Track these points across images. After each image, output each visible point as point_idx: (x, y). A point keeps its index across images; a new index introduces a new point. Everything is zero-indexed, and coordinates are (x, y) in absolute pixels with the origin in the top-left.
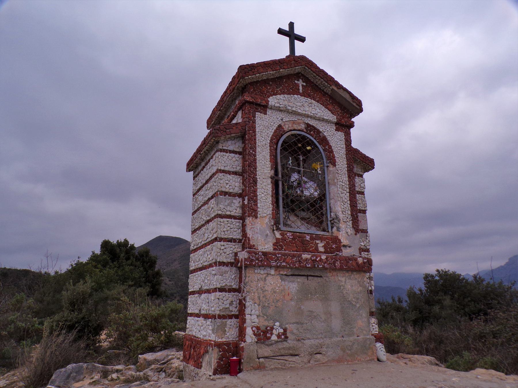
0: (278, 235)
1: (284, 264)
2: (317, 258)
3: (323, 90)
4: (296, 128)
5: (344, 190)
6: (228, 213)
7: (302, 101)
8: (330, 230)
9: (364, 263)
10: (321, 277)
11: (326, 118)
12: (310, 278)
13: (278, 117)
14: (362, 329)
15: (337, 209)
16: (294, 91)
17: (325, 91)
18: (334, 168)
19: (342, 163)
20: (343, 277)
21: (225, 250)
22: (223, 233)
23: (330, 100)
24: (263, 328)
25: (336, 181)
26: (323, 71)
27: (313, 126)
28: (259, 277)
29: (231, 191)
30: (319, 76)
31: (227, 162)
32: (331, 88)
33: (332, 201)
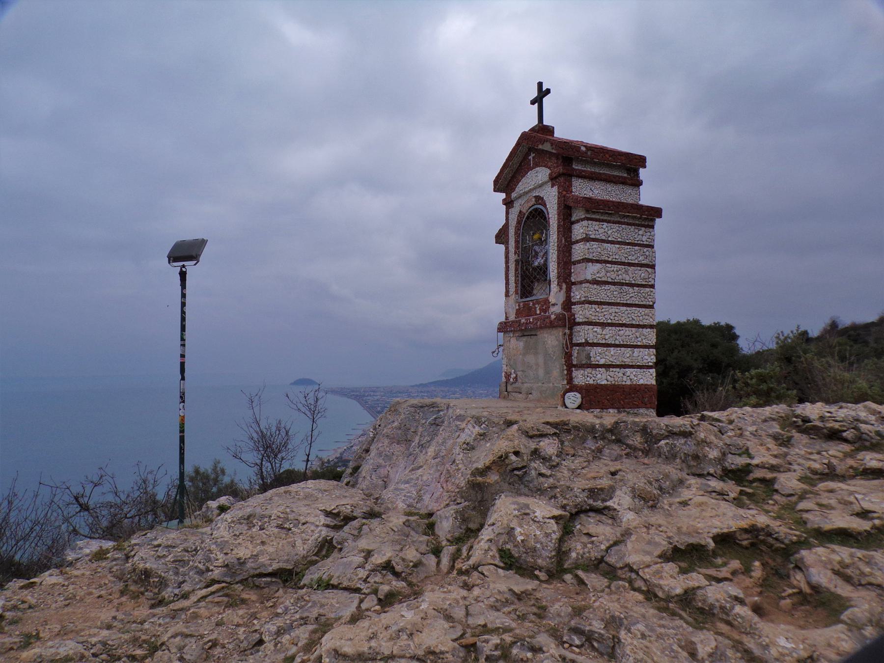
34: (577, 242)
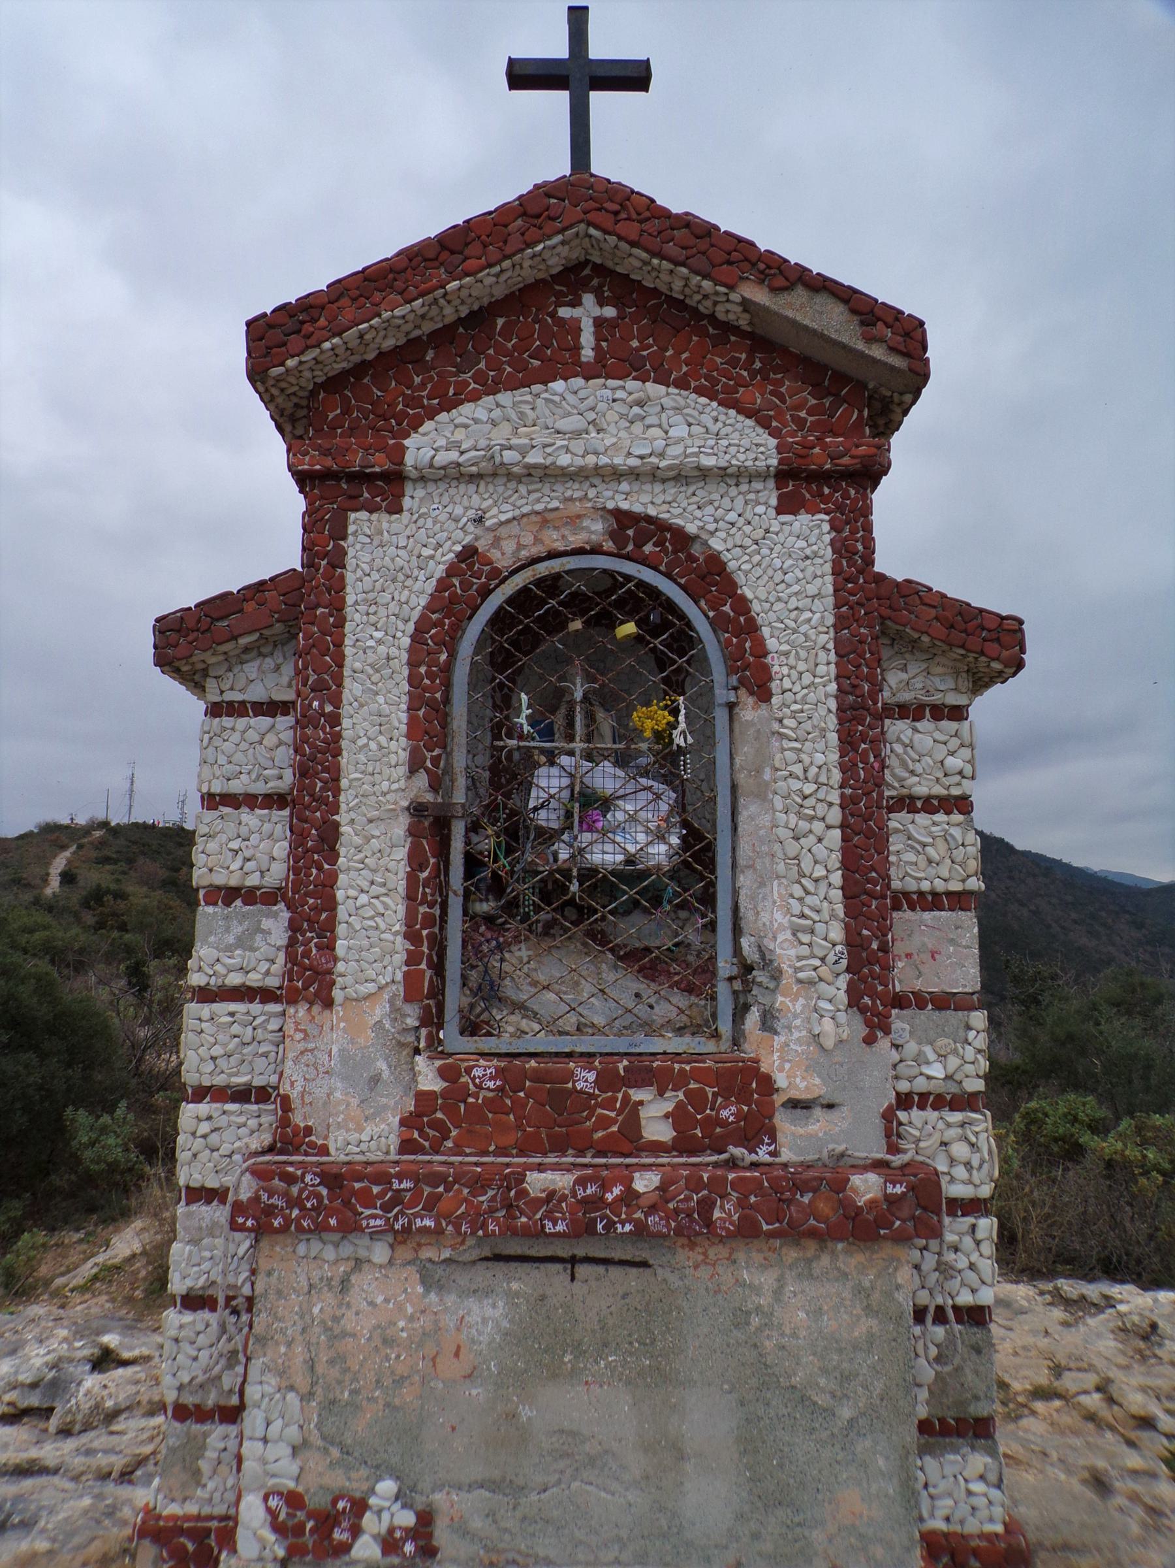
0: (429, 1080)
1: (428, 1222)
2: (605, 1186)
3: (712, 318)
4: (560, 546)
5: (812, 818)
6: (235, 979)
7: (590, 402)
8: (725, 1027)
9: (891, 1200)
10: (644, 1264)
11: (708, 461)
12: (582, 1270)
13: (458, 511)
14: (861, 1536)
15: (765, 917)
16: (559, 361)
17: (721, 316)
18: (763, 711)
19: (807, 679)
20: (763, 1268)
21: (214, 1138)
22: (209, 1067)
23: (751, 360)
24: (316, 1501)
25: (767, 775)
26: (687, 222)
27: (649, 519)
28: (316, 1275)
29: (253, 880)
30: (663, 257)
31: (239, 757)
32: (735, 297)
33: (745, 881)
34: (907, 803)
